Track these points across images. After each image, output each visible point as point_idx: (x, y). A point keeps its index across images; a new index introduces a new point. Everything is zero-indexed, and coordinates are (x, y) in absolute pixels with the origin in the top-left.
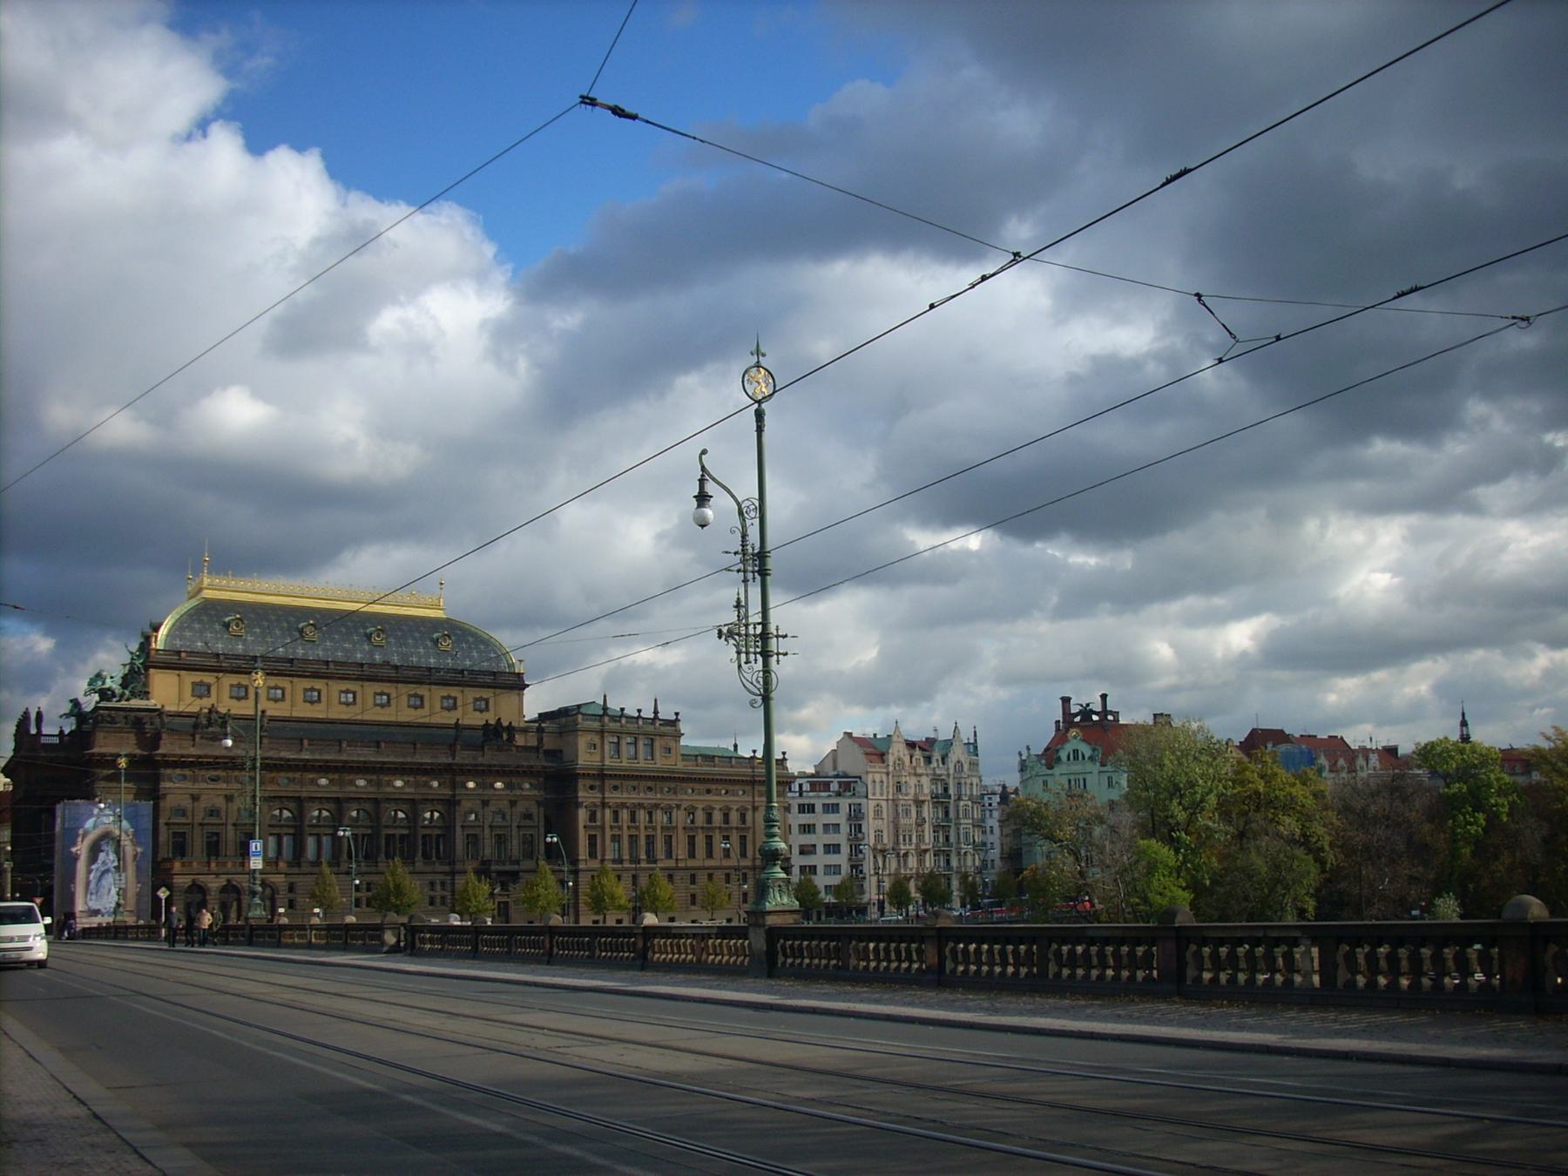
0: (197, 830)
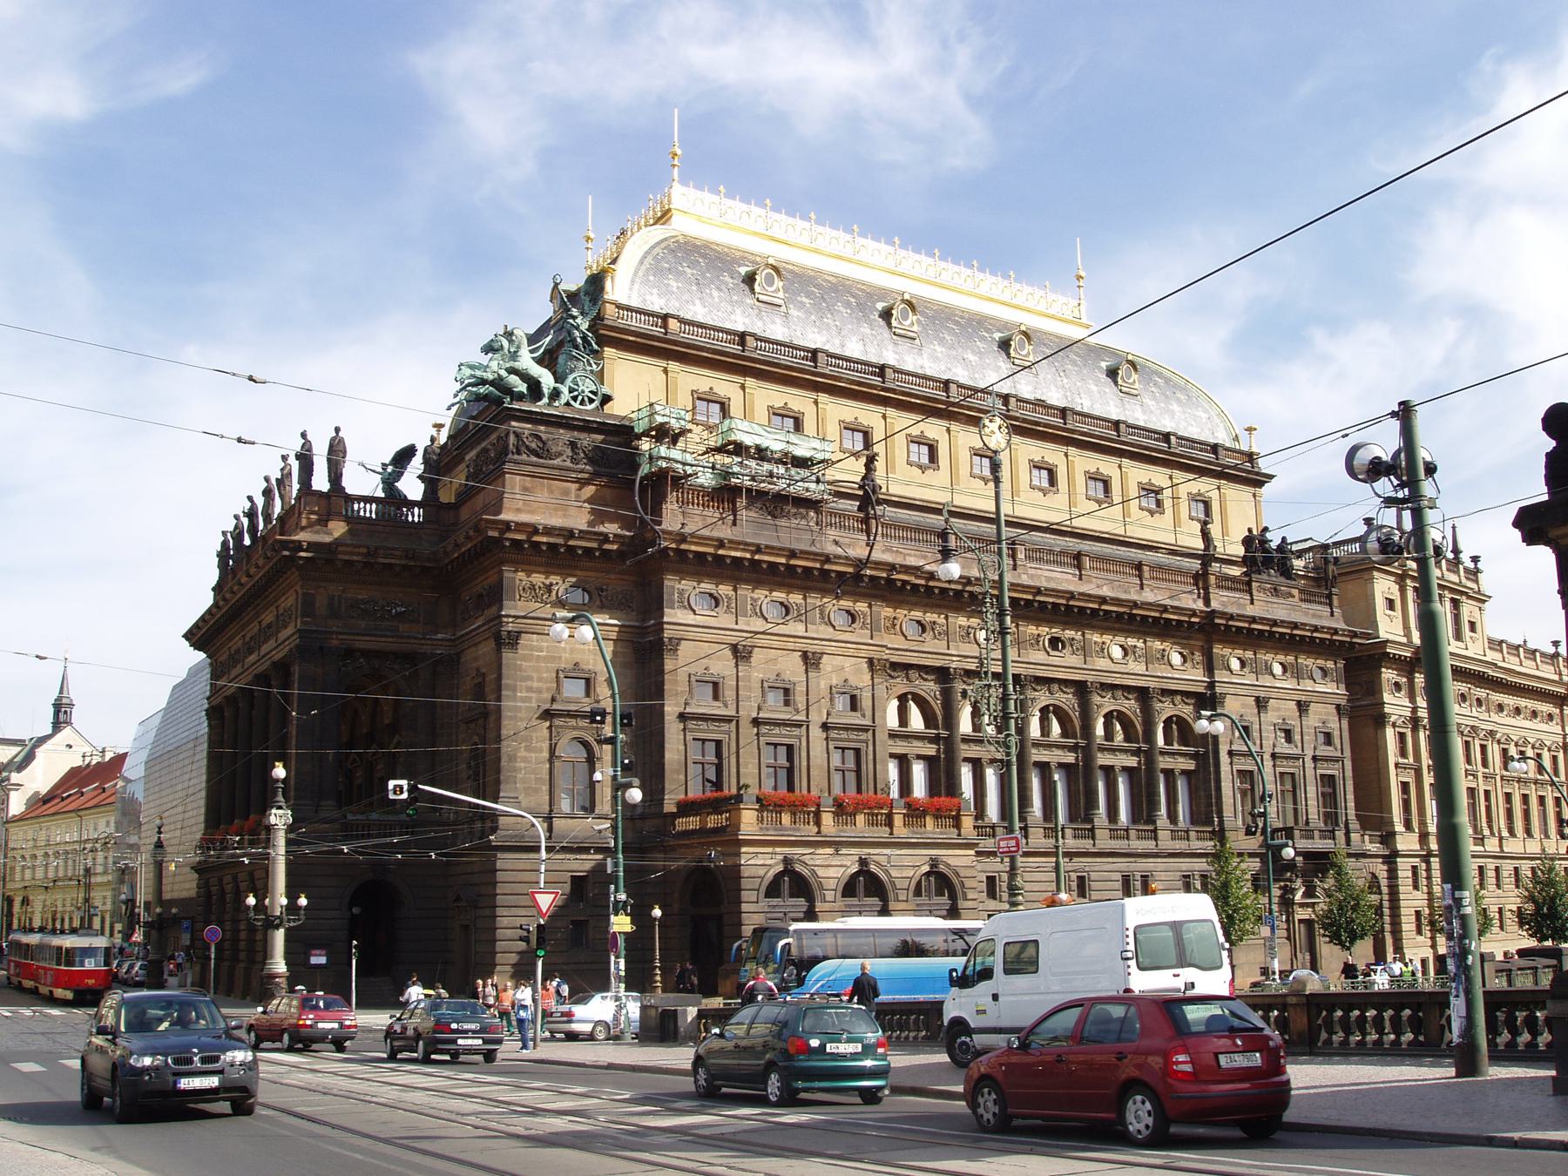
0: (748, 732)
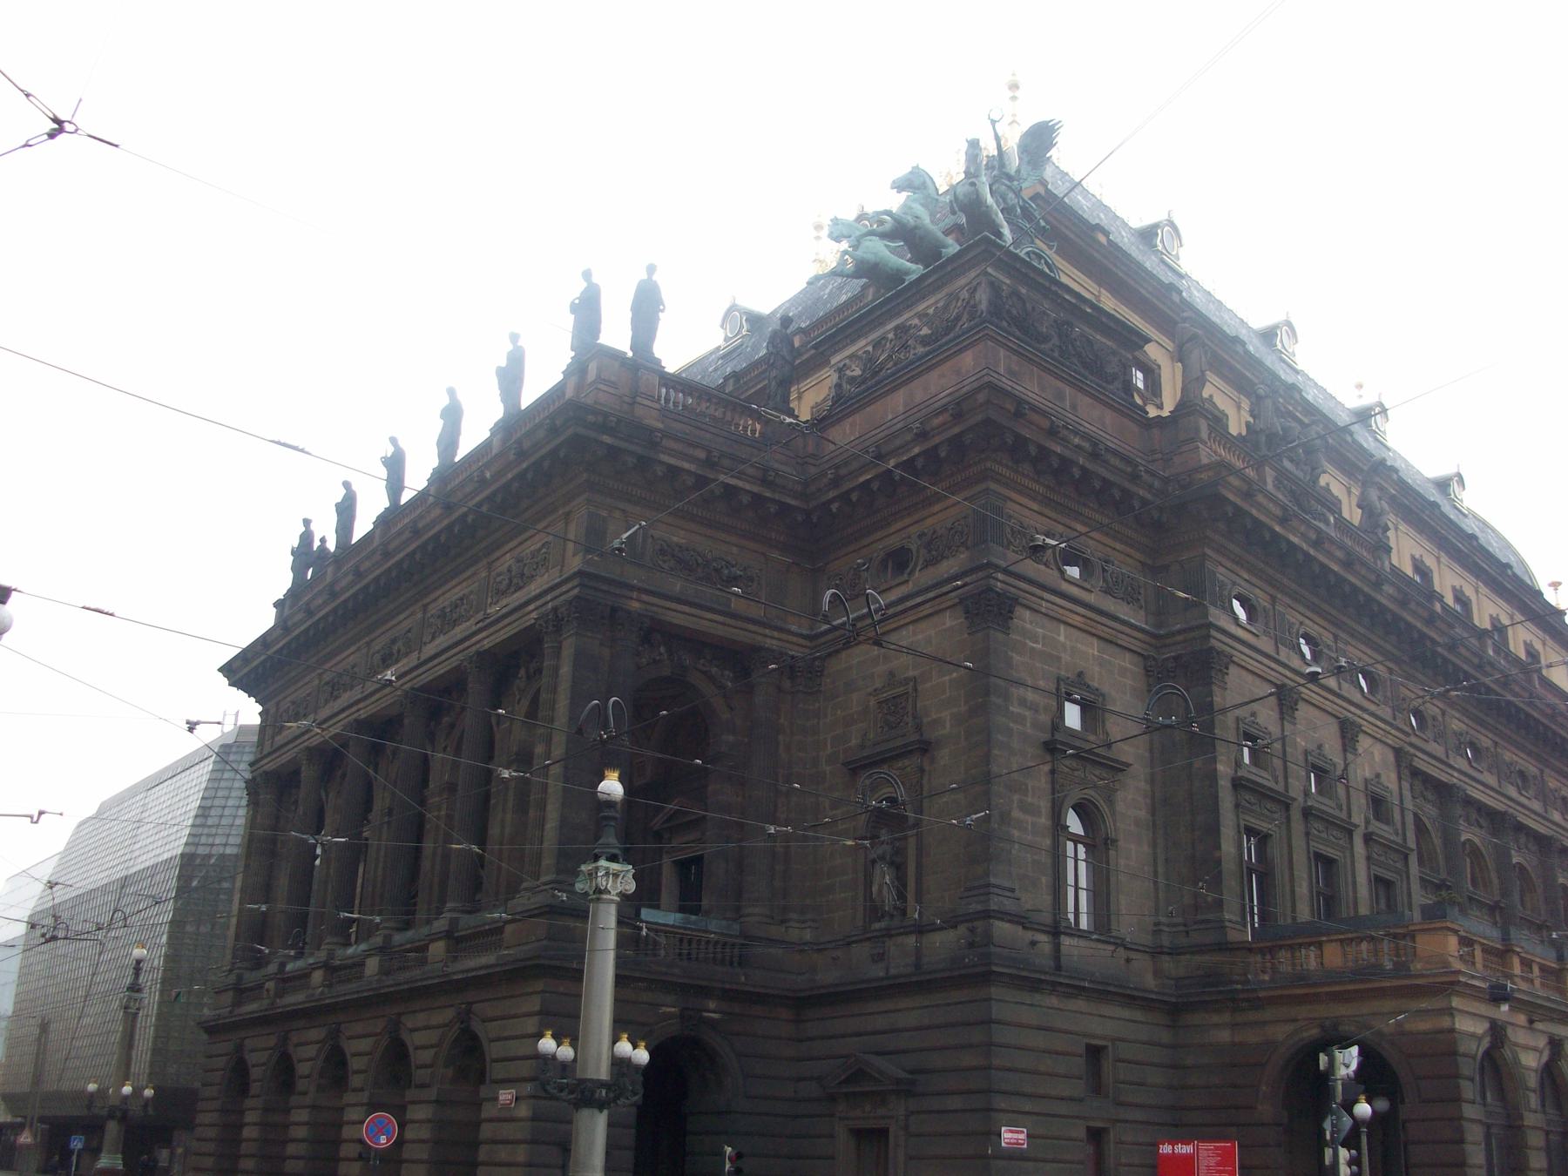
0: (1298, 826)
